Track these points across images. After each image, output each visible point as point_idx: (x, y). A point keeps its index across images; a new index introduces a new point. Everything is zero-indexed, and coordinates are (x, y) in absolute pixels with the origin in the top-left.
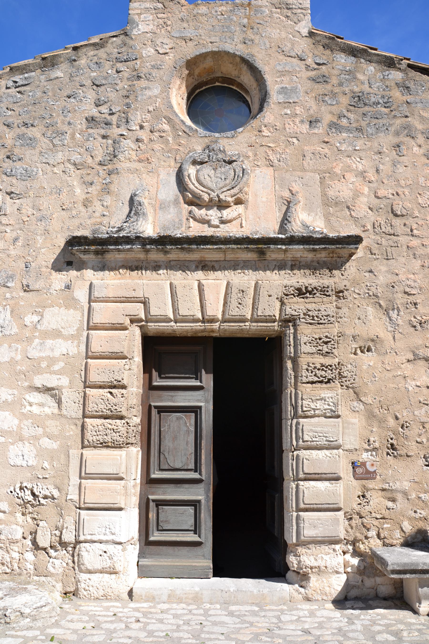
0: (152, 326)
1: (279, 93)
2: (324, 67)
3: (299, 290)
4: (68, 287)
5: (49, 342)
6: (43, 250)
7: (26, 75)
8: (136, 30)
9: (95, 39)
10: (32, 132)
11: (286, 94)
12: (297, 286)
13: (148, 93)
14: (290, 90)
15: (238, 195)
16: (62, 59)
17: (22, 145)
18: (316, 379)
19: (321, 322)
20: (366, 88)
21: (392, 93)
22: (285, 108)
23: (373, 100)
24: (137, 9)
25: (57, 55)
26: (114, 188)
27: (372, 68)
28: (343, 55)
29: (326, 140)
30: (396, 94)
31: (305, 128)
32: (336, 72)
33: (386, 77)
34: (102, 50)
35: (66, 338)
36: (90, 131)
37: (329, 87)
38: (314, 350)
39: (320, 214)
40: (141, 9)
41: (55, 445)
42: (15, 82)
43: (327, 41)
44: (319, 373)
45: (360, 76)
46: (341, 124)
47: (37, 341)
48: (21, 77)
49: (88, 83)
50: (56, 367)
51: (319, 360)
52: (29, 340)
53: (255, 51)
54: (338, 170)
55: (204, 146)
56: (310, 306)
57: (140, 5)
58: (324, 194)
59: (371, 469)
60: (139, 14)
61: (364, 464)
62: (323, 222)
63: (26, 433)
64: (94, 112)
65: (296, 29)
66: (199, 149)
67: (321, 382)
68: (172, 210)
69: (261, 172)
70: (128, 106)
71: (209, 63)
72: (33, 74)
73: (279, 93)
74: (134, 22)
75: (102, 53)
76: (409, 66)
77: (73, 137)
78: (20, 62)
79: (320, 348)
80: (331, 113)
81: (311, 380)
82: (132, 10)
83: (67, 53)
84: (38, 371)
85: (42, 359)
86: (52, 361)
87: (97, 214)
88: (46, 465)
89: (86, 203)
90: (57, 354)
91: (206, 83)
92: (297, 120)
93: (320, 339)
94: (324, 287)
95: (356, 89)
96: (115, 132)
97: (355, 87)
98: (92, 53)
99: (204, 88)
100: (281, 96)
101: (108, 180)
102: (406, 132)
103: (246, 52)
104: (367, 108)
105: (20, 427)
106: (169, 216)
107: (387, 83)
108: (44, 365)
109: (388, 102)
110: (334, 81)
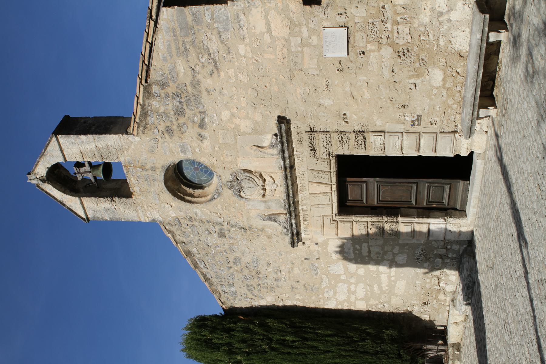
0: (335, 210)
1: (185, 154)
2: (160, 130)
3: (311, 150)
4: (316, 244)
6: (298, 254)
7: (198, 262)
8: (159, 219)
9: (170, 235)
10: (231, 260)
11: (185, 151)
12: (309, 151)
13: (199, 214)
14: (182, 148)
15: (258, 177)
16: (185, 249)
17: (240, 263)
18: (363, 145)
19: (330, 141)
20: (170, 107)
21: (170, 93)
22: (195, 151)
23: (178, 104)
24: (144, 218)
25: (184, 251)
26: (260, 227)
27: (154, 103)
28: (149, 118)
29: (213, 131)
30: (170, 90)
31: (207, 143)
32: (162, 123)
33: (158, 95)
34: (175, 232)
36: (227, 236)
37: (175, 127)
38: (346, 145)
39: (263, 136)
40: (144, 216)
42: (203, 267)
43: (141, 128)
44: (360, 142)
45: (162, 109)
46: (199, 121)
48: (200, 264)
51: (352, 142)
53: (159, 166)
54: (233, 126)
55: (228, 190)
56: (321, 146)
57: (142, 217)
58: (249, 134)
59: (416, 117)
60: (148, 217)
61: (413, 122)
62: (268, 135)
64: (216, 236)
65: (136, 143)
66: (230, 192)
67: (365, 142)
68: (270, 204)
69: (240, 164)
70: (209, 222)
71: (169, 184)
72: (197, 260)
73: (185, 154)
74: (153, 220)
75: (177, 233)
76: (146, 82)
77: (233, 244)
78: (190, 263)
79: (345, 142)
80: (193, 128)
81: (364, 147)
82: (146, 220)
83: (181, 247)
84: (361, 253)
85: (354, 252)
86: (355, 249)
87: (276, 233)
89: (269, 237)
90: (352, 248)
91: (179, 177)
92: (201, 144)
93: (340, 141)
94: (309, 139)
95: (172, 113)
96: (225, 226)
97: (171, 114)
98: (178, 237)
99: (181, 177)
100: (188, 153)
101: (256, 230)
102: (197, 86)
103: (161, 169)
104: (185, 108)
105: (388, 260)
106: (274, 205)
107: (163, 95)
108: (357, 252)
109: (177, 95)
110: (169, 124)
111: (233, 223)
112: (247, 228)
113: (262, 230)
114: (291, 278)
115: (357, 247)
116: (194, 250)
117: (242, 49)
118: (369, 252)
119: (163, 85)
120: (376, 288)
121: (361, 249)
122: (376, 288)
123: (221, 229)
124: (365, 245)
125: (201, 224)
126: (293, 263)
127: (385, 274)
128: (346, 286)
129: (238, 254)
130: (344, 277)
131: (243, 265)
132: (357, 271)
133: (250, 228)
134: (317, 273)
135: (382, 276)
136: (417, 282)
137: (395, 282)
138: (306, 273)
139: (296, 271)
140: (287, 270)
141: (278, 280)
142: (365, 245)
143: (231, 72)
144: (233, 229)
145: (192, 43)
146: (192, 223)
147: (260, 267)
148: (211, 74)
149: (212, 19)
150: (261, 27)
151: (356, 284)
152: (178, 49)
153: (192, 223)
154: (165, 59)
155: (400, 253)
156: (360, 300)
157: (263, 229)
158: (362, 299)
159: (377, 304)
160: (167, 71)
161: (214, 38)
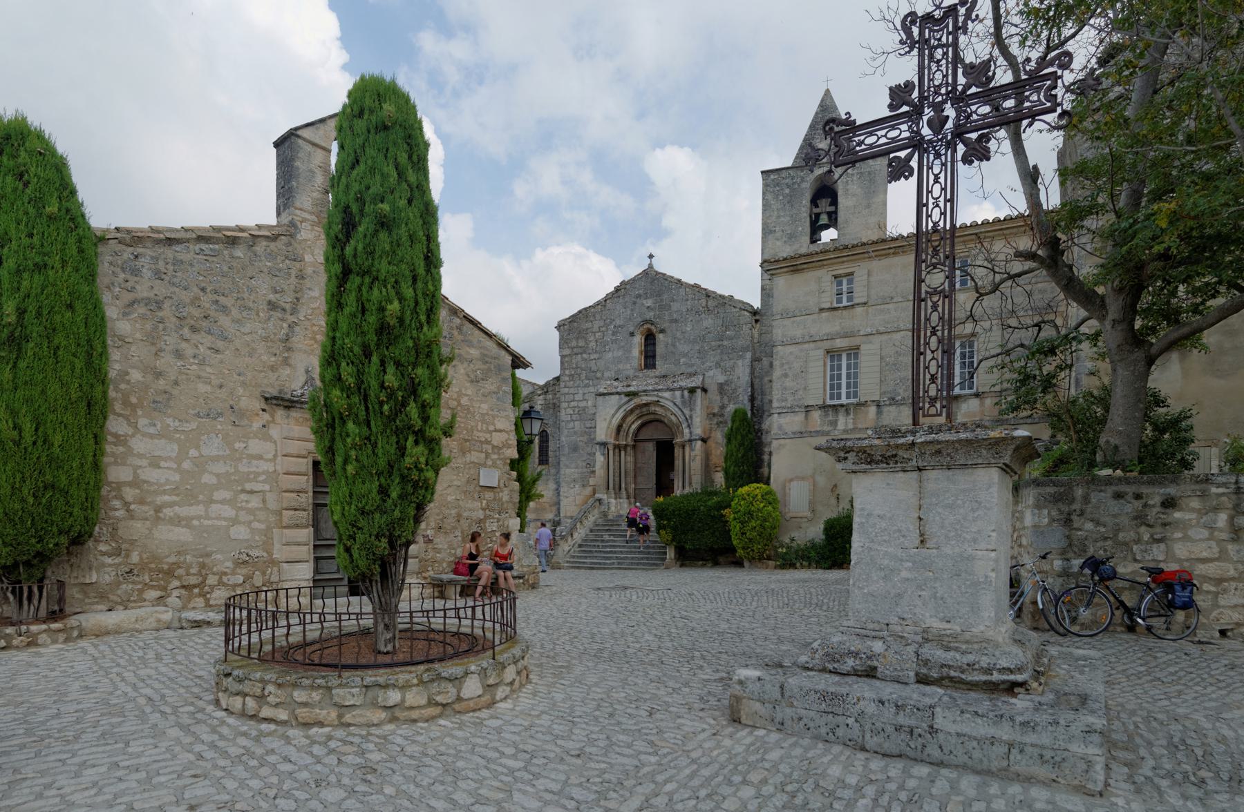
4: (264, 426)
5: (254, 462)
13: (312, 294)
17: (217, 310)
26: (292, 362)
30: (455, 332)
35: (267, 460)
36: (272, 313)
41: (263, 526)
47: (245, 460)
49: (265, 270)
50: (262, 478)
52: (240, 459)
63: (242, 519)
64: (272, 297)
70: (297, 299)
77: (258, 314)
84: (249, 480)
85: (251, 473)
86: (258, 474)
88: (257, 538)
90: (261, 470)
105: (237, 515)
108: (252, 476)
111: (297, 329)
112: (288, 345)
113: (286, 362)
114: (184, 377)
115: (262, 478)
116: (239, 252)
117: (485, 406)
118: (252, 492)
119: (459, 328)
120: (166, 498)
121: (260, 482)
122: (166, 498)
123: (284, 310)
124: (267, 487)
125: (292, 287)
126: (221, 387)
127: (206, 511)
128: (174, 455)
129: (235, 312)
130: (193, 453)
131: (212, 313)
132: (211, 473)
133: (289, 349)
134: (200, 417)
135: (201, 507)
136: (188, 557)
137: (188, 526)
138: (201, 400)
139: (203, 388)
140: (203, 374)
141: (178, 354)
142: (267, 487)
143: (469, 392)
144: (285, 325)
145: (489, 370)
146: (293, 275)
147: (210, 337)
148: (469, 376)
149: (505, 392)
150: (499, 426)
151: (178, 470)
152: (486, 355)
153: (293, 275)
154: (479, 342)
155: (253, 531)
156: (135, 472)
157: (289, 365)
158: (136, 475)
159: (122, 498)
160: (470, 337)
161: (493, 388)
